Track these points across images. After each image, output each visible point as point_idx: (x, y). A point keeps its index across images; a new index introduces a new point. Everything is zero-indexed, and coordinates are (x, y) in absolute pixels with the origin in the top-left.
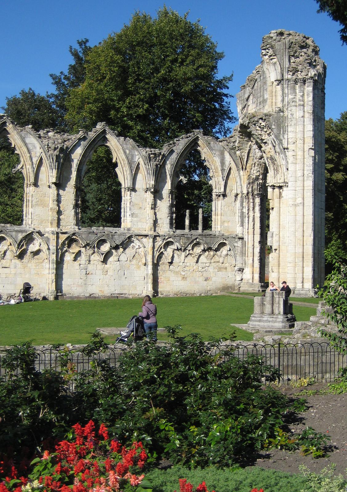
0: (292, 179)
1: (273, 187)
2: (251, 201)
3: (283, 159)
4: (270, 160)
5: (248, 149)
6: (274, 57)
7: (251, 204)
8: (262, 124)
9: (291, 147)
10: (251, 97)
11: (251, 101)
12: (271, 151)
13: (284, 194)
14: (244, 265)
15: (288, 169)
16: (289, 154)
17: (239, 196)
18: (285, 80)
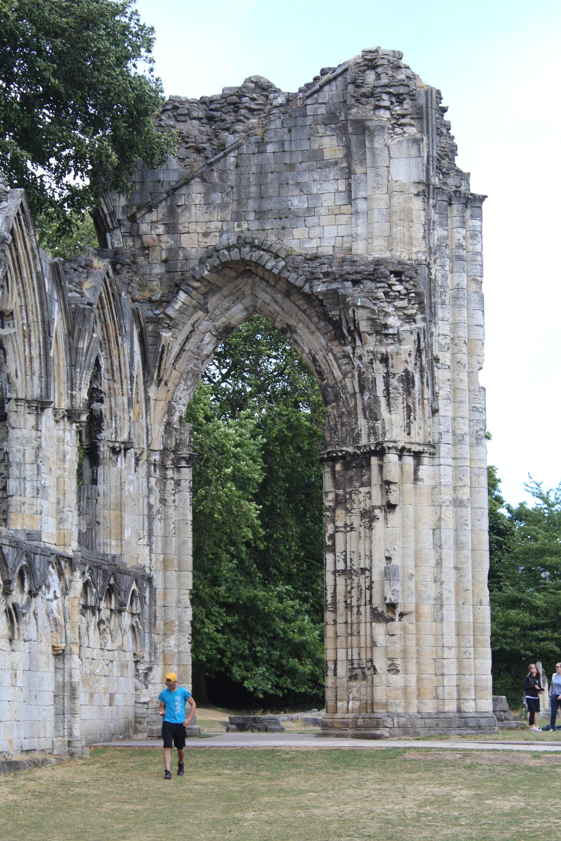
0: (448, 438)
1: (401, 452)
2: (170, 473)
3: (428, 385)
4: (401, 380)
5: (188, 328)
6: (413, 122)
7: (170, 485)
8: (394, 288)
9: (445, 358)
10: (197, 187)
11: (198, 199)
12: (409, 360)
13: (425, 471)
14: (153, 659)
15: (435, 411)
16: (441, 375)
17: (144, 457)
18: (431, 187)
